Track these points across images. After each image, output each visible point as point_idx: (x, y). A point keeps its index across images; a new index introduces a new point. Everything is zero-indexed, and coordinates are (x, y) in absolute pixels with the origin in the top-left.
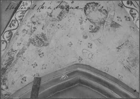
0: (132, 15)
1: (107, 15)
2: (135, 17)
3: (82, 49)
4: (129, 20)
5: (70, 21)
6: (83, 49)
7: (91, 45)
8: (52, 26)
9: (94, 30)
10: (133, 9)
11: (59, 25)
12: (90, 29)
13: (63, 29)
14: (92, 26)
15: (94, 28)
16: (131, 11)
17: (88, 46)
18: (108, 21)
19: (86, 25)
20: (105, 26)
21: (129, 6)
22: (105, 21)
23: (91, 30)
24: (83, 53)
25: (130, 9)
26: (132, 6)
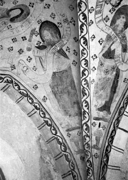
0: (82, 53)
1: (59, 40)
2: (84, 56)
3: (19, 59)
4: (76, 55)
5: (22, 27)
6: (21, 60)
7: (31, 59)
8: (4, 24)
9: (40, 48)
10: (85, 49)
11: (10, 25)
12: (37, 44)
13: (11, 32)
14: (41, 43)
15: (41, 45)
16: (83, 50)
17: (27, 59)
18: (57, 46)
19: (36, 39)
20: (52, 48)
21: (84, 45)
22: (54, 44)
23: (37, 46)
24: (19, 63)
25: (83, 48)
26: (86, 47)
